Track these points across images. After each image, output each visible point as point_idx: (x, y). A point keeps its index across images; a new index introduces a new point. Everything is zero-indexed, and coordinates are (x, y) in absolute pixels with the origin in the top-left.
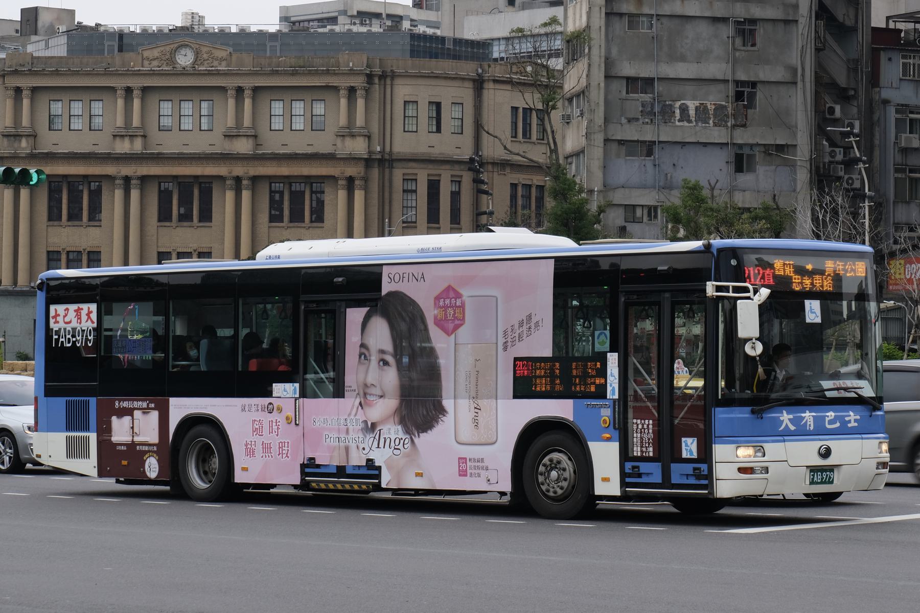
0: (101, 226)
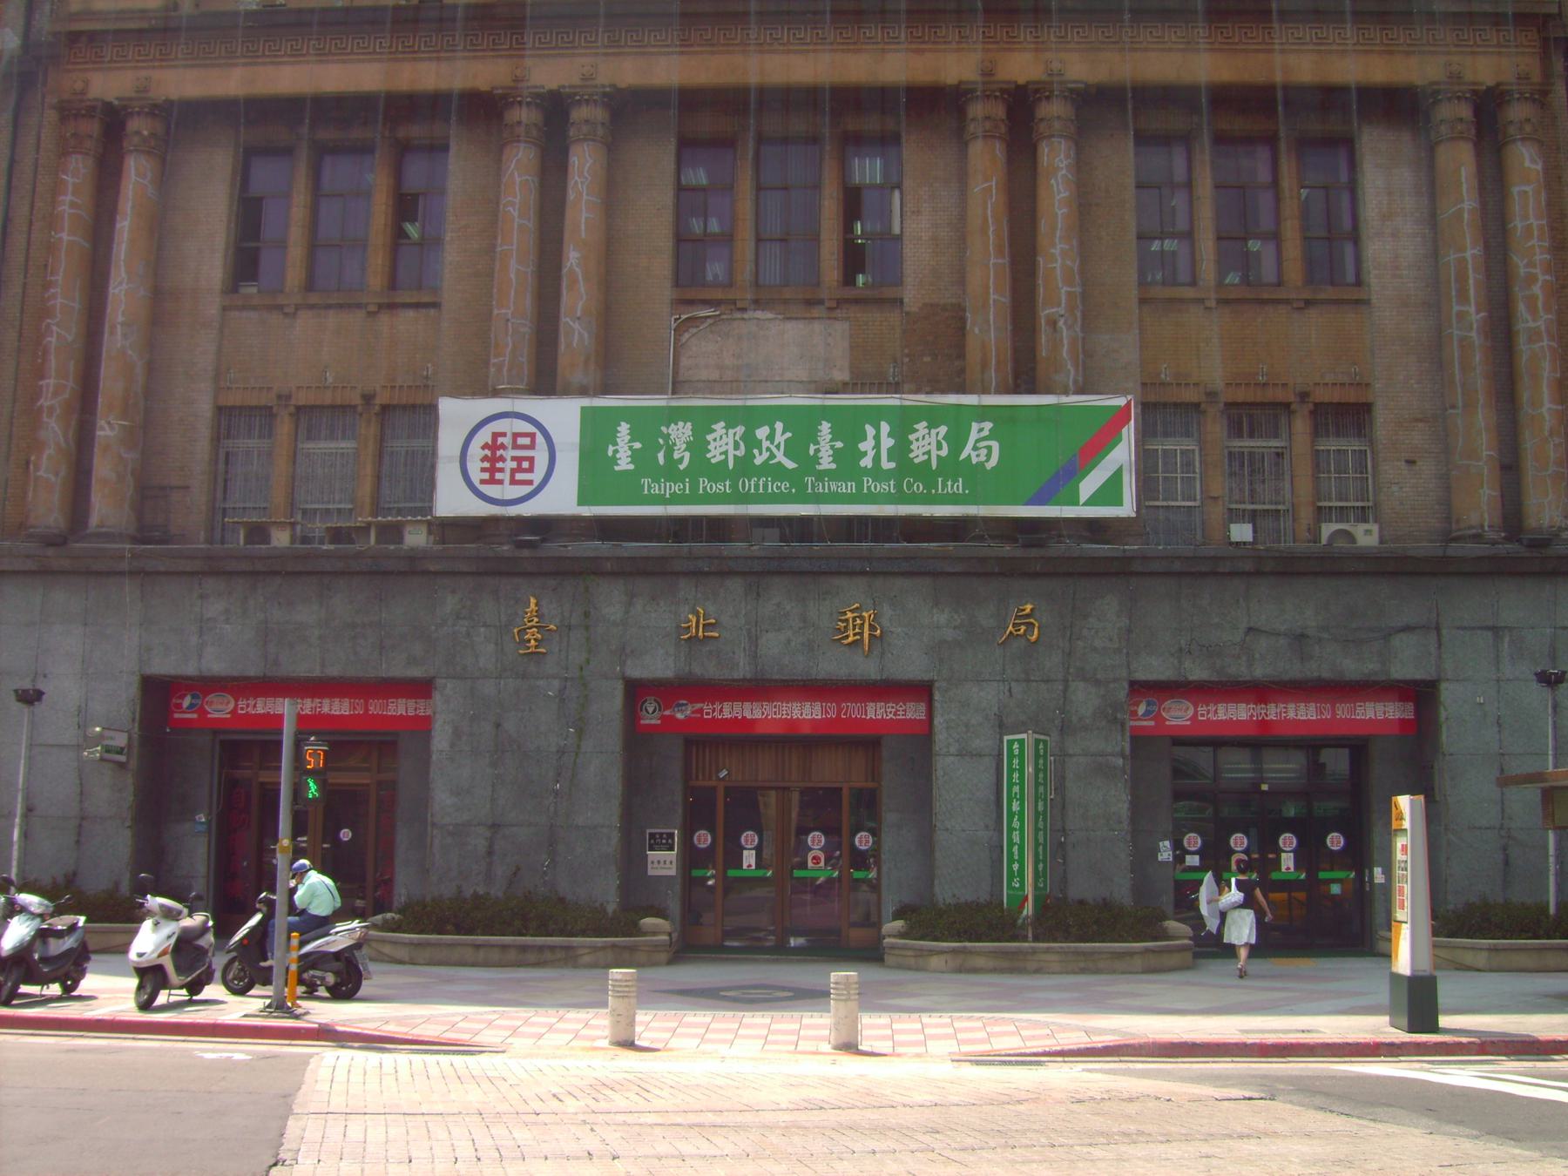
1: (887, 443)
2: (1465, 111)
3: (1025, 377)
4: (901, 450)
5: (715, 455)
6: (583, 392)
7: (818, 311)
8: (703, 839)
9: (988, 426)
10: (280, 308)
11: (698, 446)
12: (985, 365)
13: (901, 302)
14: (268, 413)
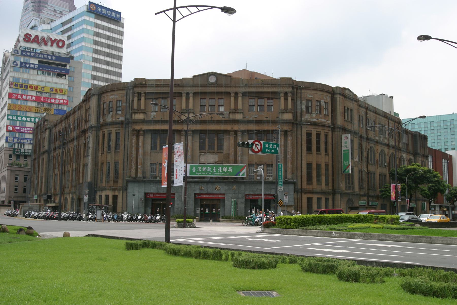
1: (221, 169)
3: (235, 162)
4: (222, 170)
5: (203, 170)
6: (190, 163)
7: (214, 154)
8: (202, 209)
9: (231, 167)
10: (157, 152)
11: (202, 169)
12: (231, 161)
13: (223, 153)
14: (156, 164)
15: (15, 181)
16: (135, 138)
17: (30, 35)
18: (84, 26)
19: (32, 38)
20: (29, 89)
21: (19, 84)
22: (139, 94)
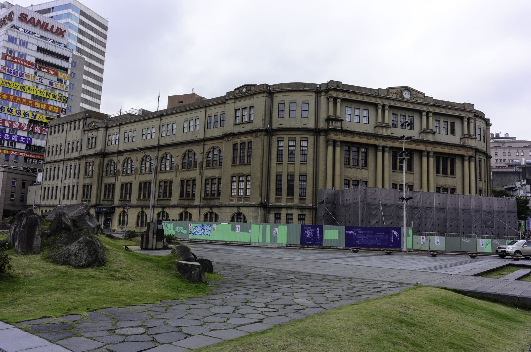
0: (368, 169)
2: (468, 158)
15: (13, 186)
16: (330, 149)
17: (27, 16)
18: (69, 20)
19: (28, 19)
20: (24, 77)
21: (12, 70)
22: (335, 99)
